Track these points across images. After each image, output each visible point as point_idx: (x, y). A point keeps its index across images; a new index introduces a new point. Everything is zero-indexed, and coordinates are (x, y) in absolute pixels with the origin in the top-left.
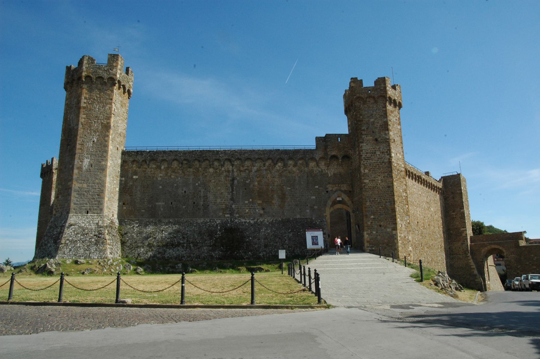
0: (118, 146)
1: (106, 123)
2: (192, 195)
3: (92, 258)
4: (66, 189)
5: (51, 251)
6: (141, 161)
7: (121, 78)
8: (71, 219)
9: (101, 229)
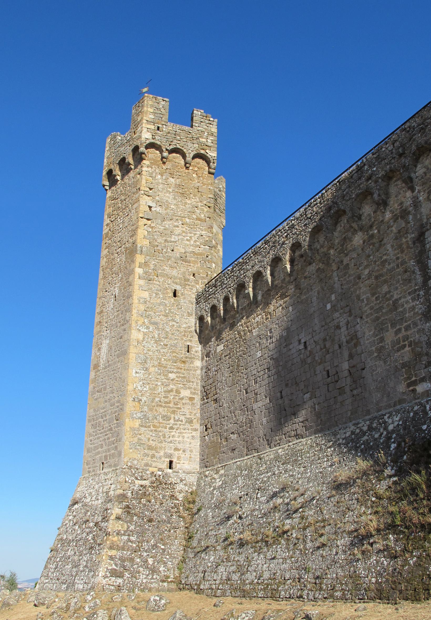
2: (321, 349)
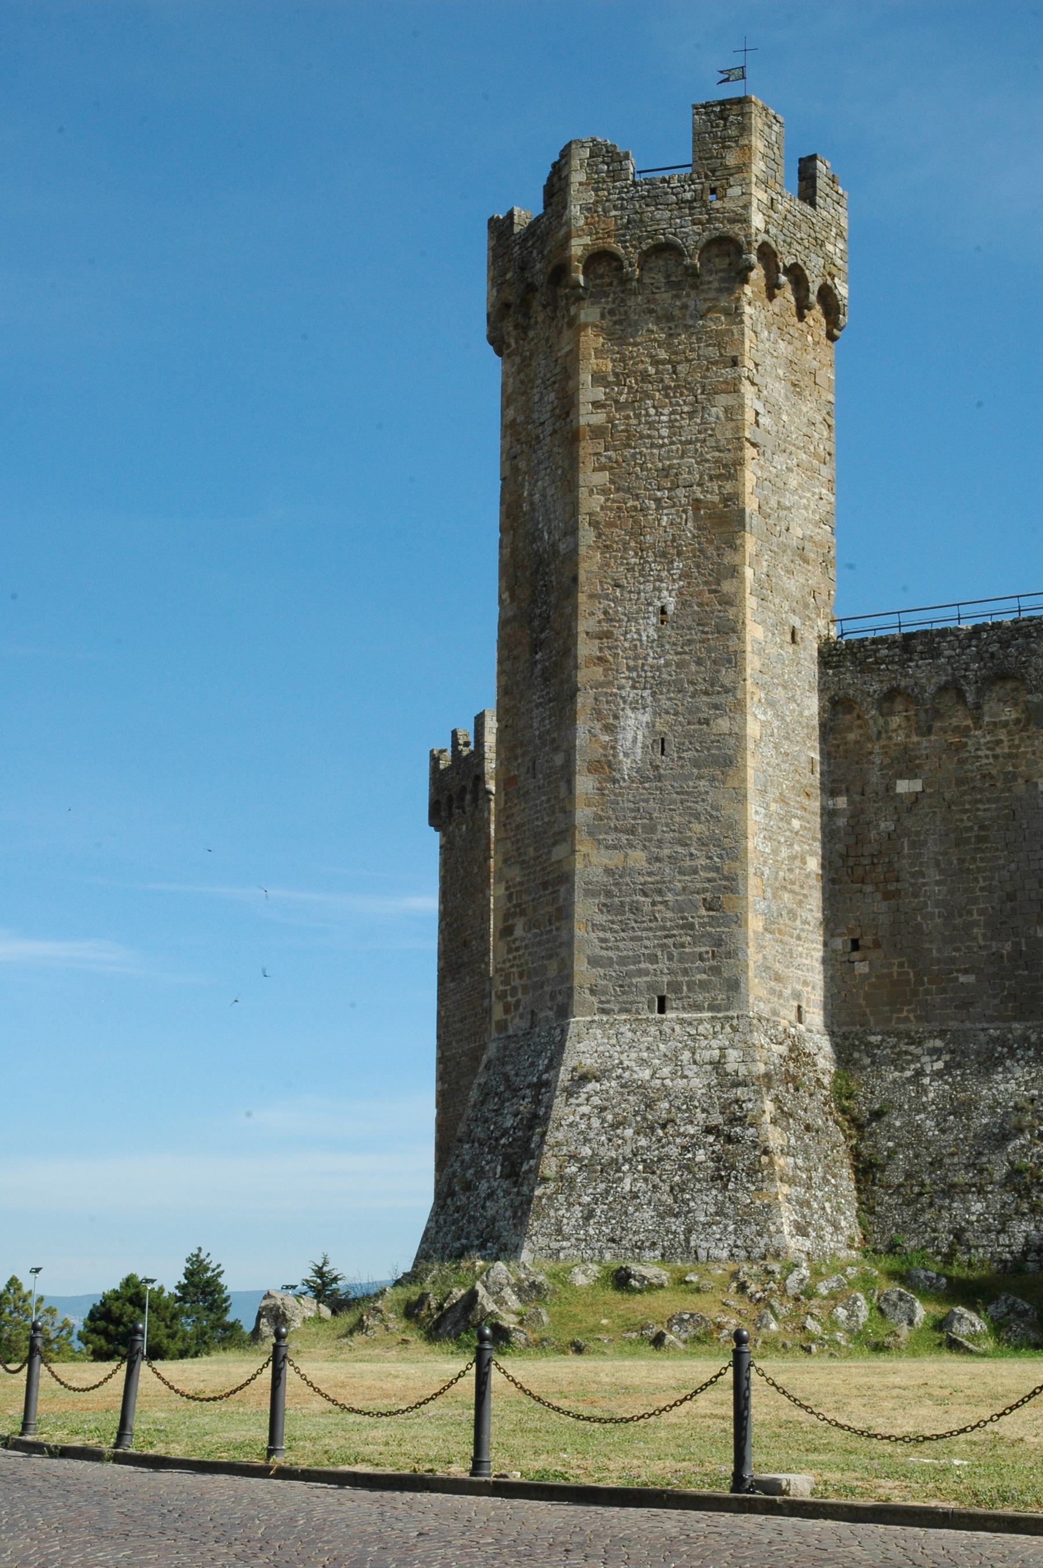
0: (796, 621)
1: (716, 499)
3: (702, 1254)
4: (545, 885)
5: (494, 1220)
6: (931, 689)
7: (773, 231)
8: (581, 1047)
9: (740, 1092)
